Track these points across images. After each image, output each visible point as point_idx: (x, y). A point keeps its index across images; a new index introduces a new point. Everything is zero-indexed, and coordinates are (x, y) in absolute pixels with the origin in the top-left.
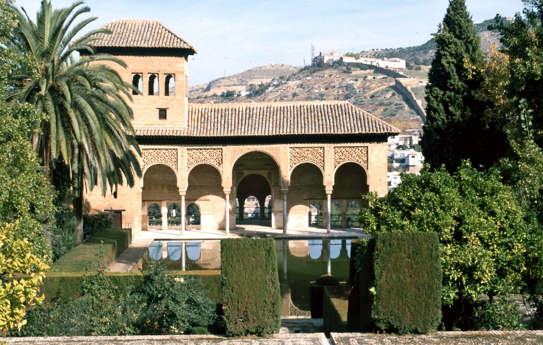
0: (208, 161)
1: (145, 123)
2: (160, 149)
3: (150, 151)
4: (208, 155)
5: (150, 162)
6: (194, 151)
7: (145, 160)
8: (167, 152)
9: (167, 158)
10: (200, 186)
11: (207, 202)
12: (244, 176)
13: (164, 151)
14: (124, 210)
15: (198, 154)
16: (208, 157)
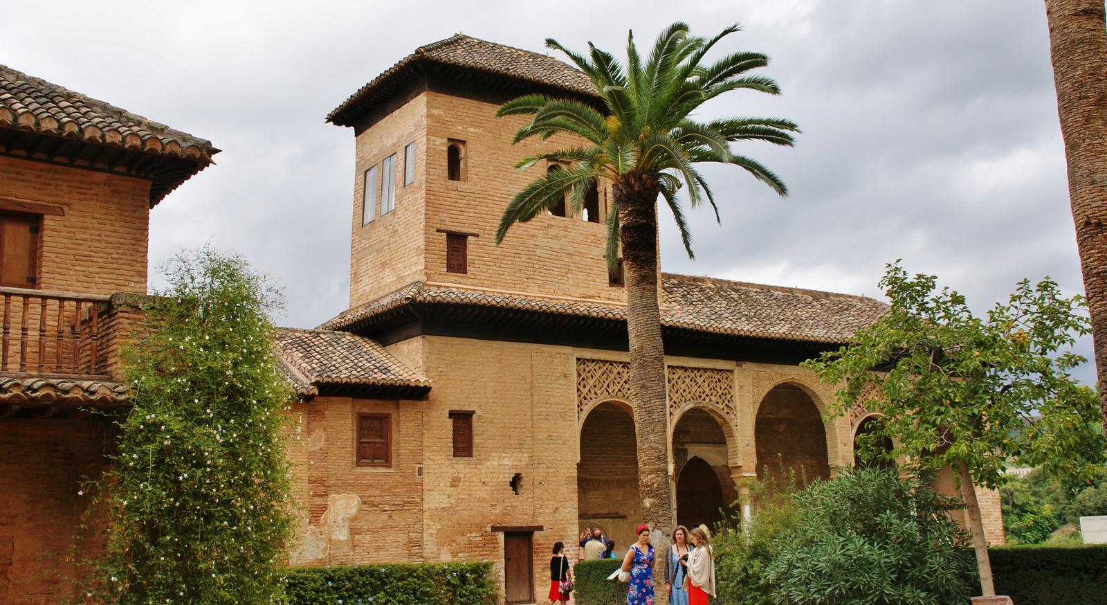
0: (707, 399)
1: (579, 291)
2: (611, 363)
3: (591, 366)
4: (706, 384)
5: (593, 395)
6: (680, 372)
7: (581, 388)
8: (626, 370)
9: (626, 386)
10: (608, 482)
11: (621, 521)
12: (688, 459)
13: (620, 369)
14: (541, 528)
15: (687, 380)
16: (707, 390)
